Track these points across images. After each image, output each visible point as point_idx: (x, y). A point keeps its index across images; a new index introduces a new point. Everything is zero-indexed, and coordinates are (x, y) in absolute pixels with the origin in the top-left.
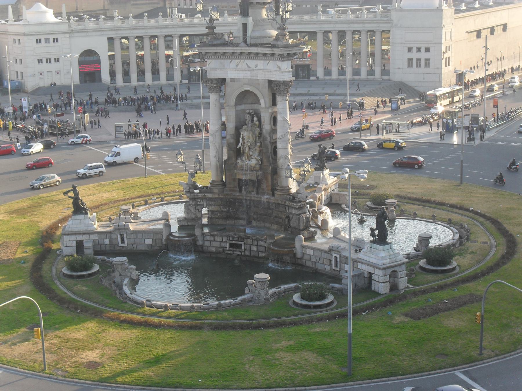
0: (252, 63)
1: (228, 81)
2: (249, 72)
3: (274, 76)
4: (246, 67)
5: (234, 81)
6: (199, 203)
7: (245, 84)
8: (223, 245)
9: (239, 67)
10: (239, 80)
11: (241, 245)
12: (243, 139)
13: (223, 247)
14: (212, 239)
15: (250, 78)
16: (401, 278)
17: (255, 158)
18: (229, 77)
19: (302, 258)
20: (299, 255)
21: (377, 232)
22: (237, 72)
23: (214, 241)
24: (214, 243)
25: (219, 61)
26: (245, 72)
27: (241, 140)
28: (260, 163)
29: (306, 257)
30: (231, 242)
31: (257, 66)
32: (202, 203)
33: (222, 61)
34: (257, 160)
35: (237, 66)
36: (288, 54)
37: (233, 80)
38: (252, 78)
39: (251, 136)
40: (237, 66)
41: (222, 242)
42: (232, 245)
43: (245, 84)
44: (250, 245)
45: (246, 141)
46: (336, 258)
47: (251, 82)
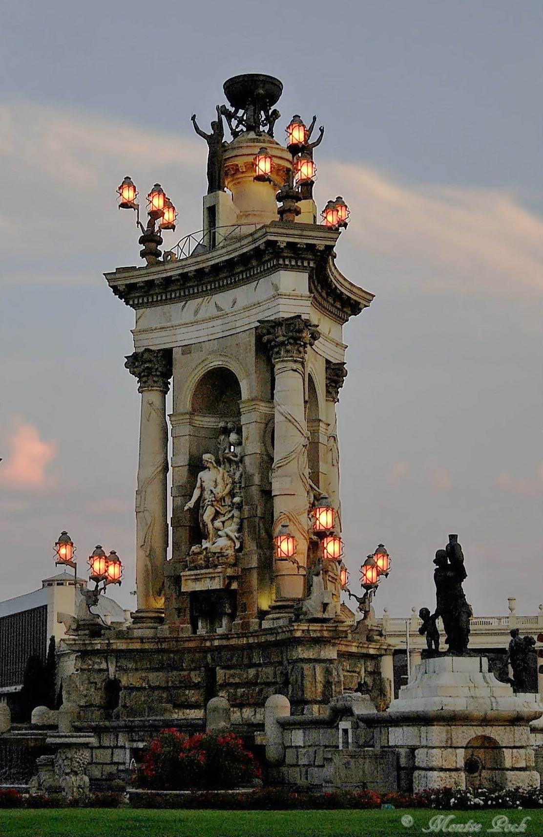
1: (177, 354)
2: (219, 322)
4: (215, 313)
6: (96, 667)
12: (202, 489)
13: (118, 764)
15: (221, 335)
16: (513, 769)
17: (227, 536)
19: (281, 762)
20: (272, 753)
21: (440, 624)
23: (101, 747)
25: (158, 310)
27: (196, 493)
28: (238, 546)
29: (290, 758)
30: (135, 745)
32: (104, 666)
33: (167, 307)
34: (230, 538)
35: (196, 312)
36: (291, 246)
37: (187, 349)
39: (219, 480)
40: (196, 312)
41: (117, 747)
45: (207, 495)
46: (345, 731)
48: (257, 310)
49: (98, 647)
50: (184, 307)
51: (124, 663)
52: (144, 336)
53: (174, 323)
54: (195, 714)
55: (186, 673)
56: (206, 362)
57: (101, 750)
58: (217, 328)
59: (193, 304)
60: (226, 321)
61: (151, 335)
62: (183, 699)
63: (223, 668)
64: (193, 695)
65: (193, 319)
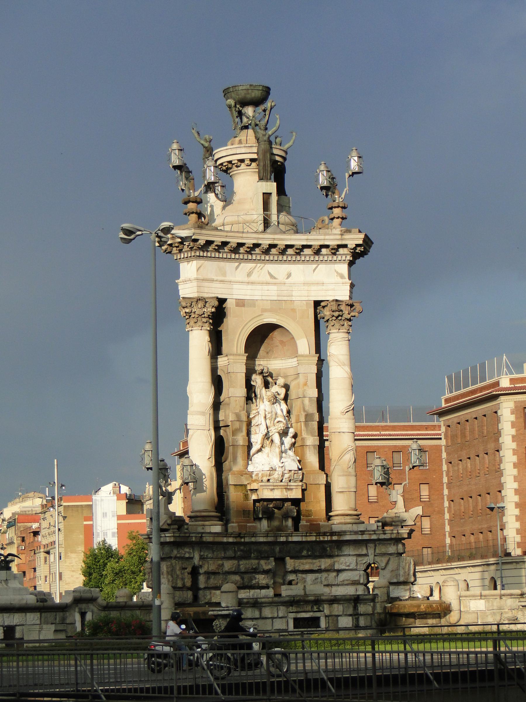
0: (279, 270)
1: (229, 305)
2: (275, 288)
3: (330, 293)
4: (268, 278)
5: (244, 306)
7: (264, 310)
8: (279, 625)
9: (254, 277)
10: (252, 303)
11: (318, 619)
14: (257, 614)
18: (235, 297)
22: (250, 287)
23: (262, 618)
24: (260, 622)
26: (266, 287)
31: (289, 275)
37: (240, 303)
38: (280, 298)
40: (249, 274)
41: (278, 617)
42: (298, 622)
43: (264, 310)
44: (338, 616)
47: (277, 305)
48: (320, 287)
49: (194, 539)
50: (237, 268)
51: (205, 553)
52: (206, 284)
53: (227, 279)
54: (243, 594)
55: (257, 561)
56: (262, 317)
57: (263, 621)
58: (271, 293)
59: (247, 266)
60: (284, 288)
61: (211, 285)
62: (254, 582)
63: (291, 558)
64: (262, 579)
65: (246, 279)
